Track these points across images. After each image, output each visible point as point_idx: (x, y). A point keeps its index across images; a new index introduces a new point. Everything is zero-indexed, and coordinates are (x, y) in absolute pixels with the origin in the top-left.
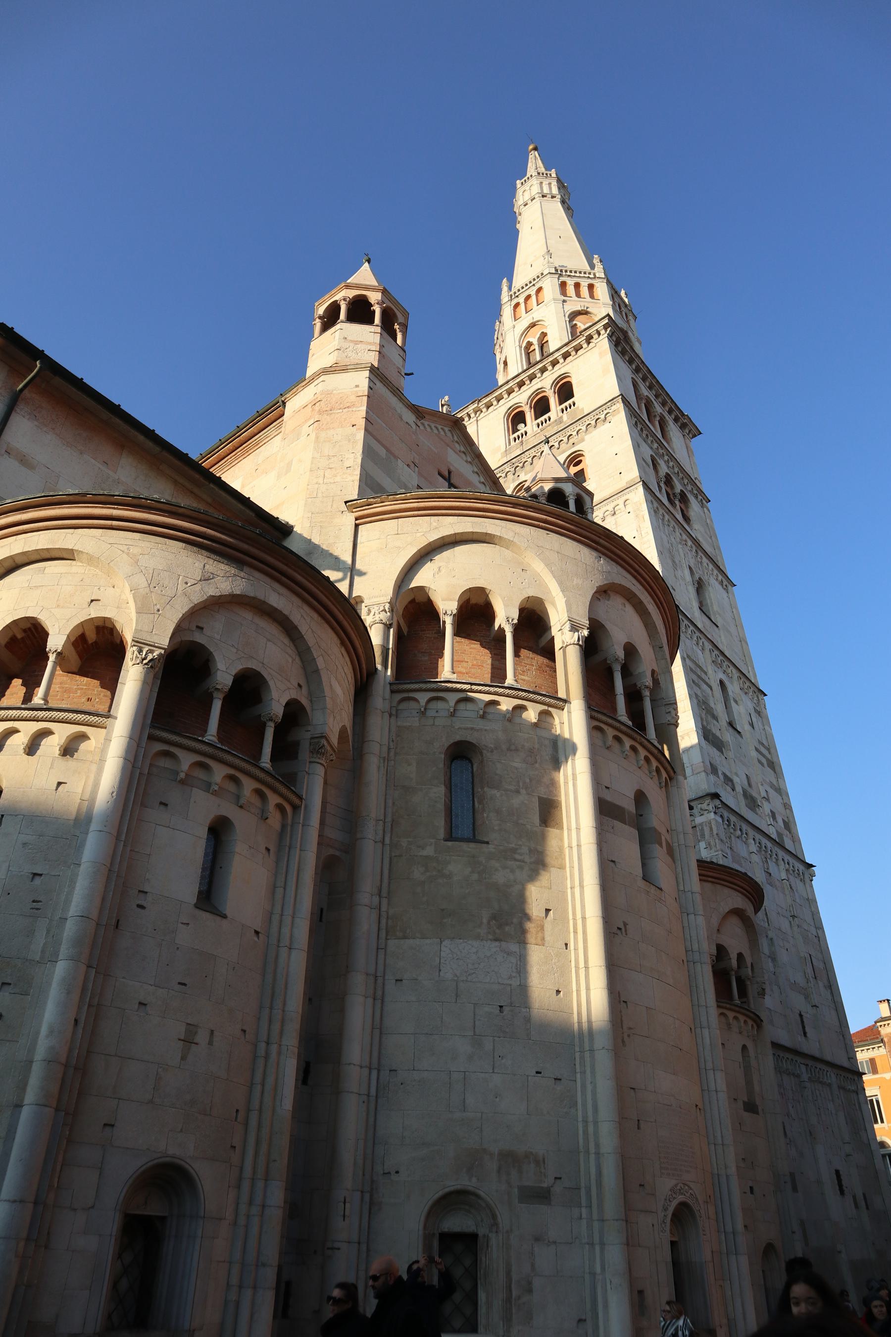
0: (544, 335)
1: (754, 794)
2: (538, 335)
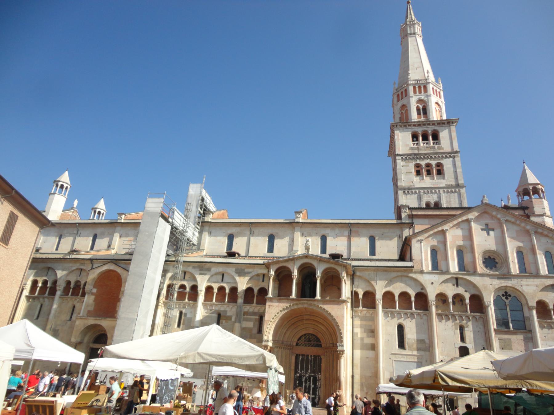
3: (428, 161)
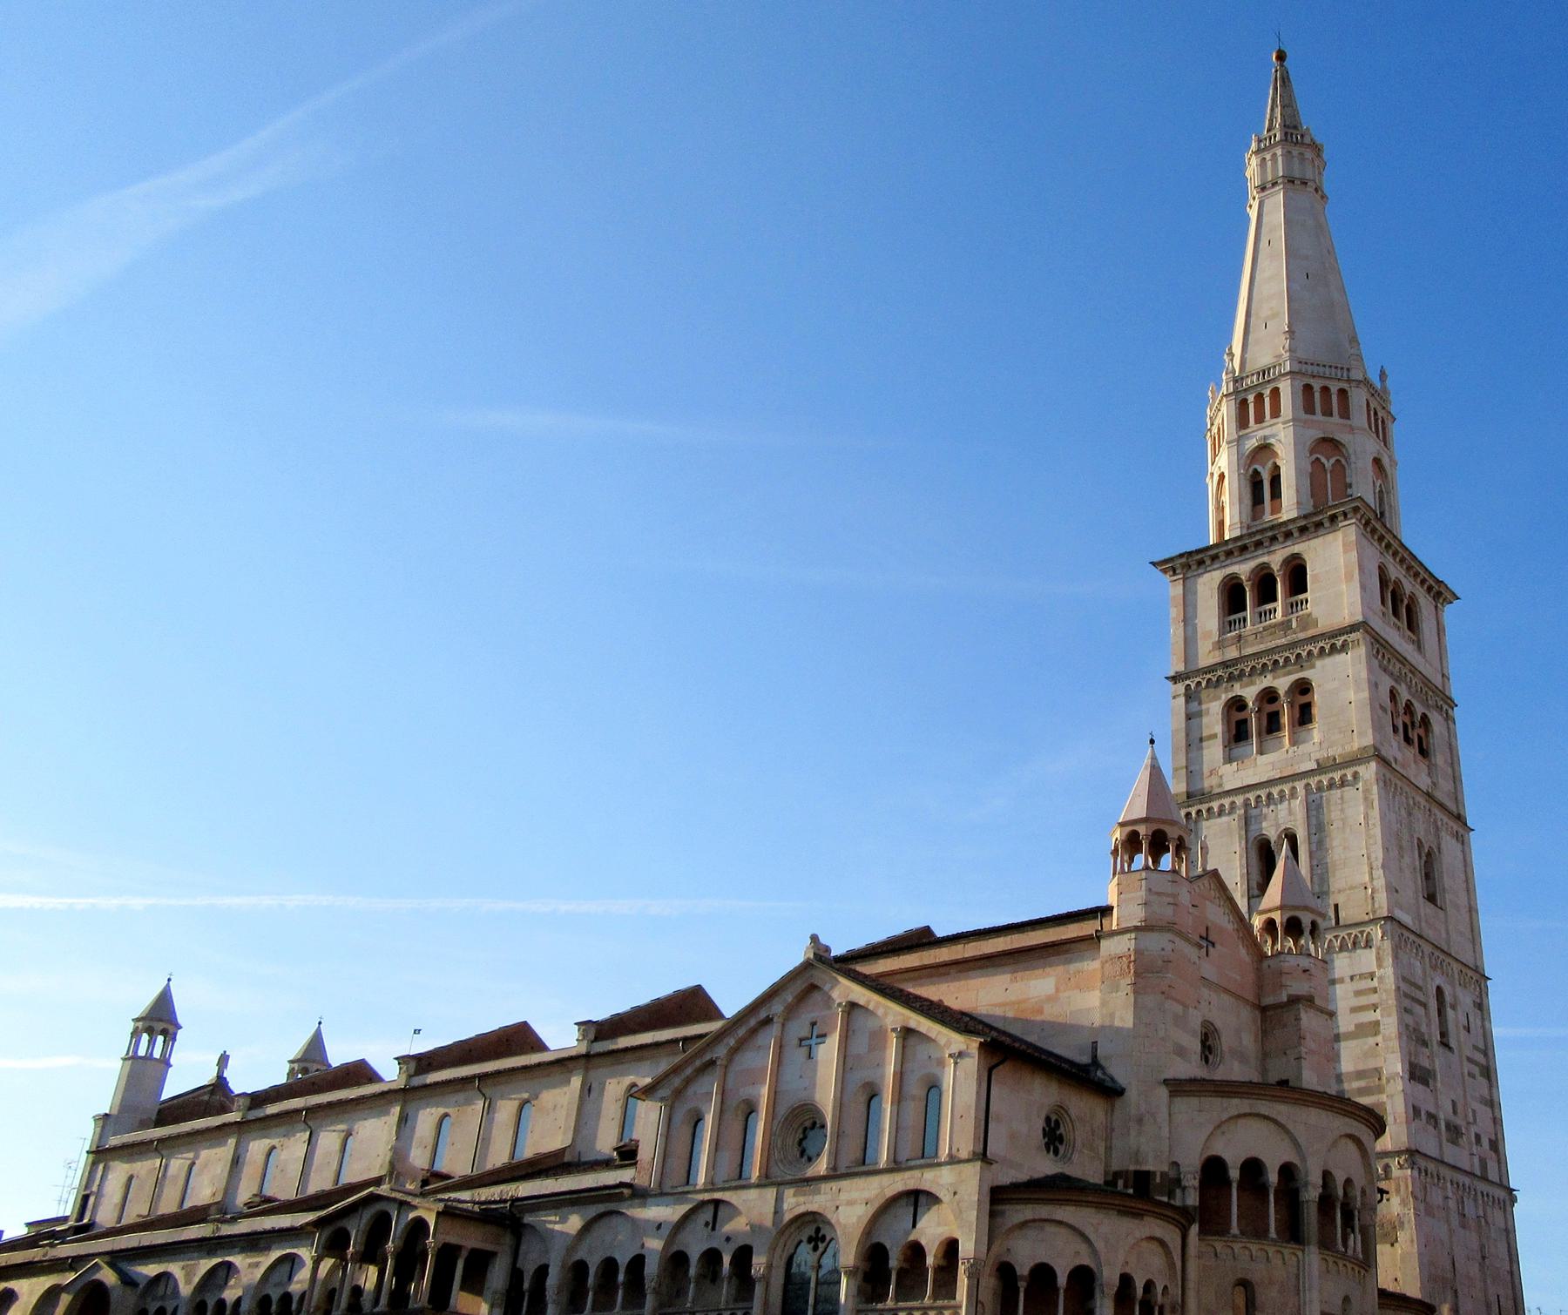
0: (1277, 468)
1: (1459, 1121)
2: (1270, 464)
3: (1266, 681)
